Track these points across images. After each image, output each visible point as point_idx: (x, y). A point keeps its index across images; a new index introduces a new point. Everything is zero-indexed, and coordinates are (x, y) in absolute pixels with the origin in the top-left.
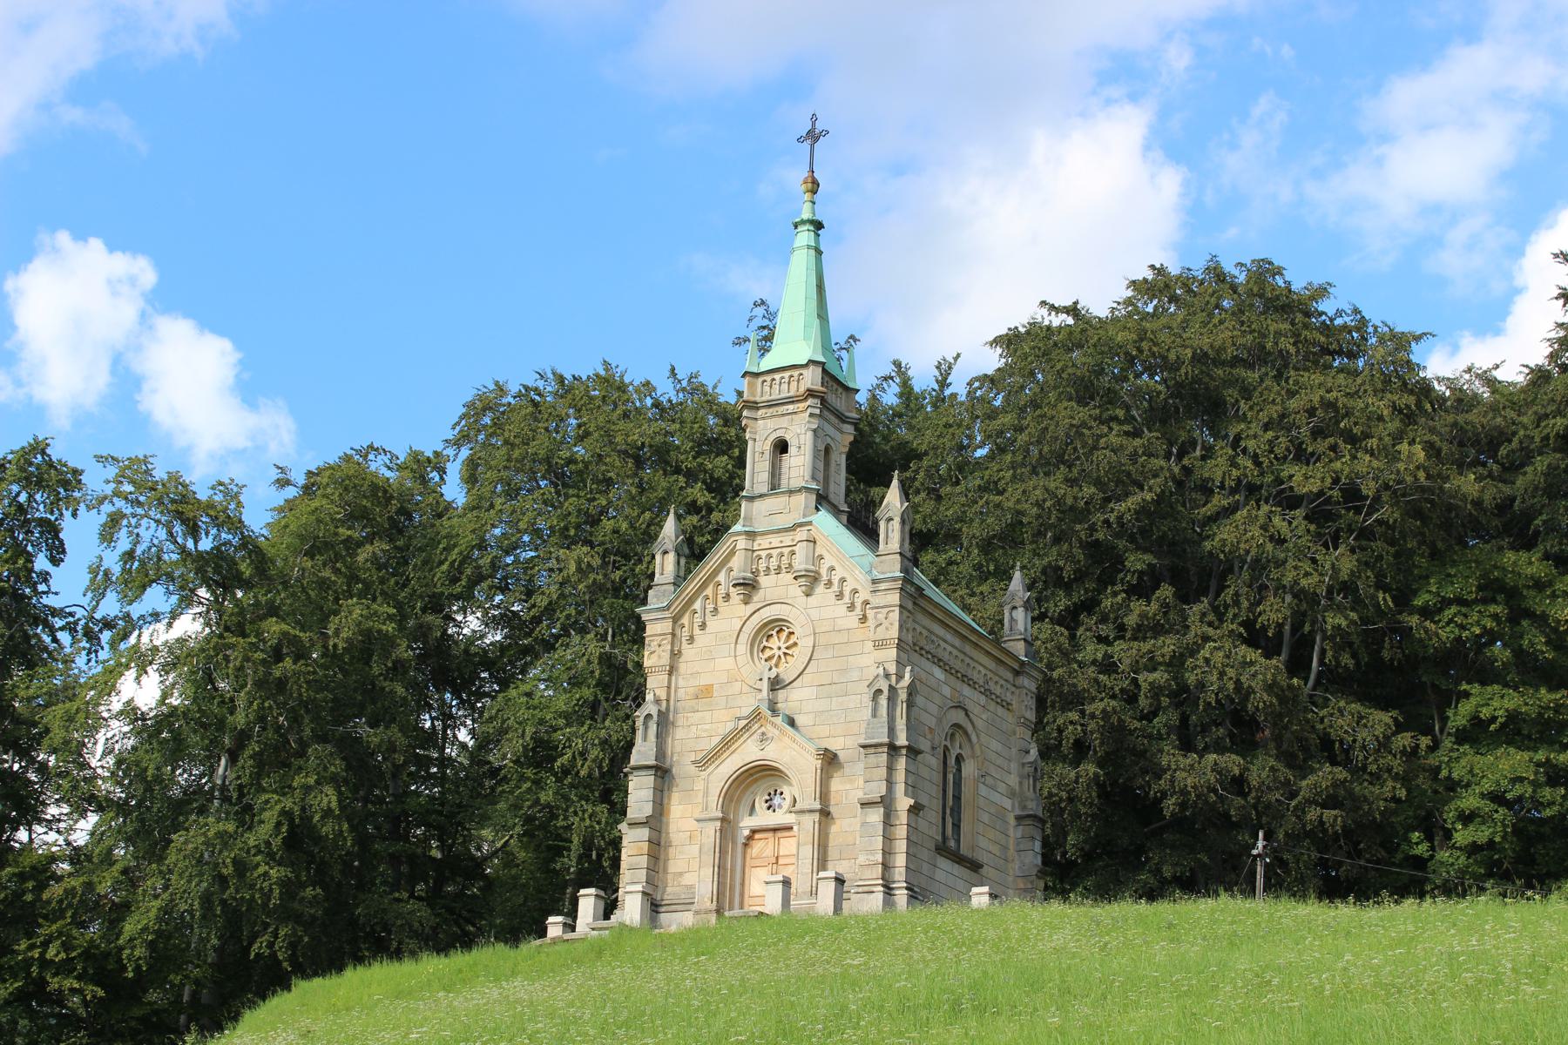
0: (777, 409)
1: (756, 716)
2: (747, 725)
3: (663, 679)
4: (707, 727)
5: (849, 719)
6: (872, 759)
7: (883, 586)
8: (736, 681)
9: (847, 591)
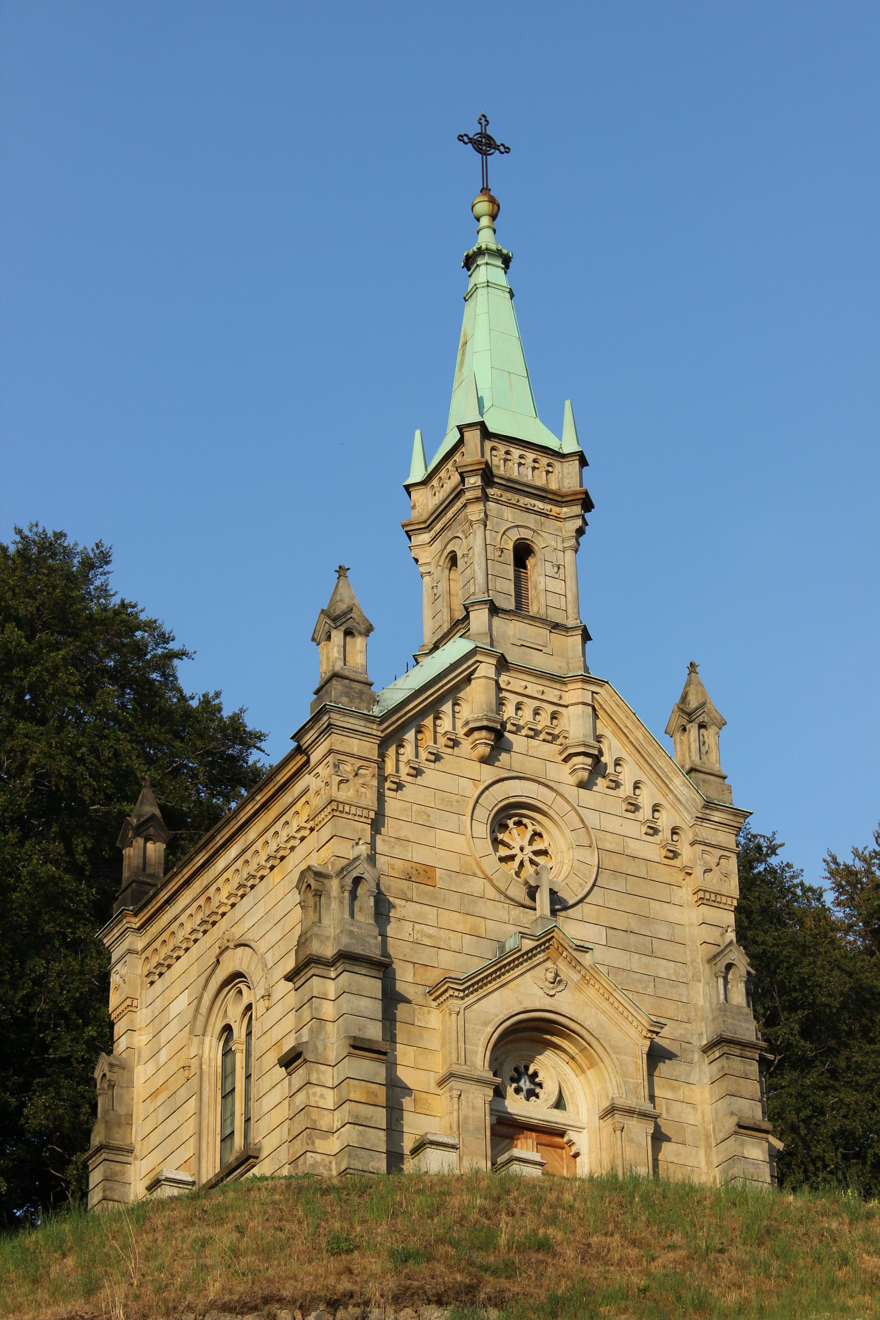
0: (517, 497)
2: (531, 950)
3: (363, 830)
4: (431, 931)
5: (660, 992)
6: (737, 1065)
7: (717, 816)
8: (474, 875)
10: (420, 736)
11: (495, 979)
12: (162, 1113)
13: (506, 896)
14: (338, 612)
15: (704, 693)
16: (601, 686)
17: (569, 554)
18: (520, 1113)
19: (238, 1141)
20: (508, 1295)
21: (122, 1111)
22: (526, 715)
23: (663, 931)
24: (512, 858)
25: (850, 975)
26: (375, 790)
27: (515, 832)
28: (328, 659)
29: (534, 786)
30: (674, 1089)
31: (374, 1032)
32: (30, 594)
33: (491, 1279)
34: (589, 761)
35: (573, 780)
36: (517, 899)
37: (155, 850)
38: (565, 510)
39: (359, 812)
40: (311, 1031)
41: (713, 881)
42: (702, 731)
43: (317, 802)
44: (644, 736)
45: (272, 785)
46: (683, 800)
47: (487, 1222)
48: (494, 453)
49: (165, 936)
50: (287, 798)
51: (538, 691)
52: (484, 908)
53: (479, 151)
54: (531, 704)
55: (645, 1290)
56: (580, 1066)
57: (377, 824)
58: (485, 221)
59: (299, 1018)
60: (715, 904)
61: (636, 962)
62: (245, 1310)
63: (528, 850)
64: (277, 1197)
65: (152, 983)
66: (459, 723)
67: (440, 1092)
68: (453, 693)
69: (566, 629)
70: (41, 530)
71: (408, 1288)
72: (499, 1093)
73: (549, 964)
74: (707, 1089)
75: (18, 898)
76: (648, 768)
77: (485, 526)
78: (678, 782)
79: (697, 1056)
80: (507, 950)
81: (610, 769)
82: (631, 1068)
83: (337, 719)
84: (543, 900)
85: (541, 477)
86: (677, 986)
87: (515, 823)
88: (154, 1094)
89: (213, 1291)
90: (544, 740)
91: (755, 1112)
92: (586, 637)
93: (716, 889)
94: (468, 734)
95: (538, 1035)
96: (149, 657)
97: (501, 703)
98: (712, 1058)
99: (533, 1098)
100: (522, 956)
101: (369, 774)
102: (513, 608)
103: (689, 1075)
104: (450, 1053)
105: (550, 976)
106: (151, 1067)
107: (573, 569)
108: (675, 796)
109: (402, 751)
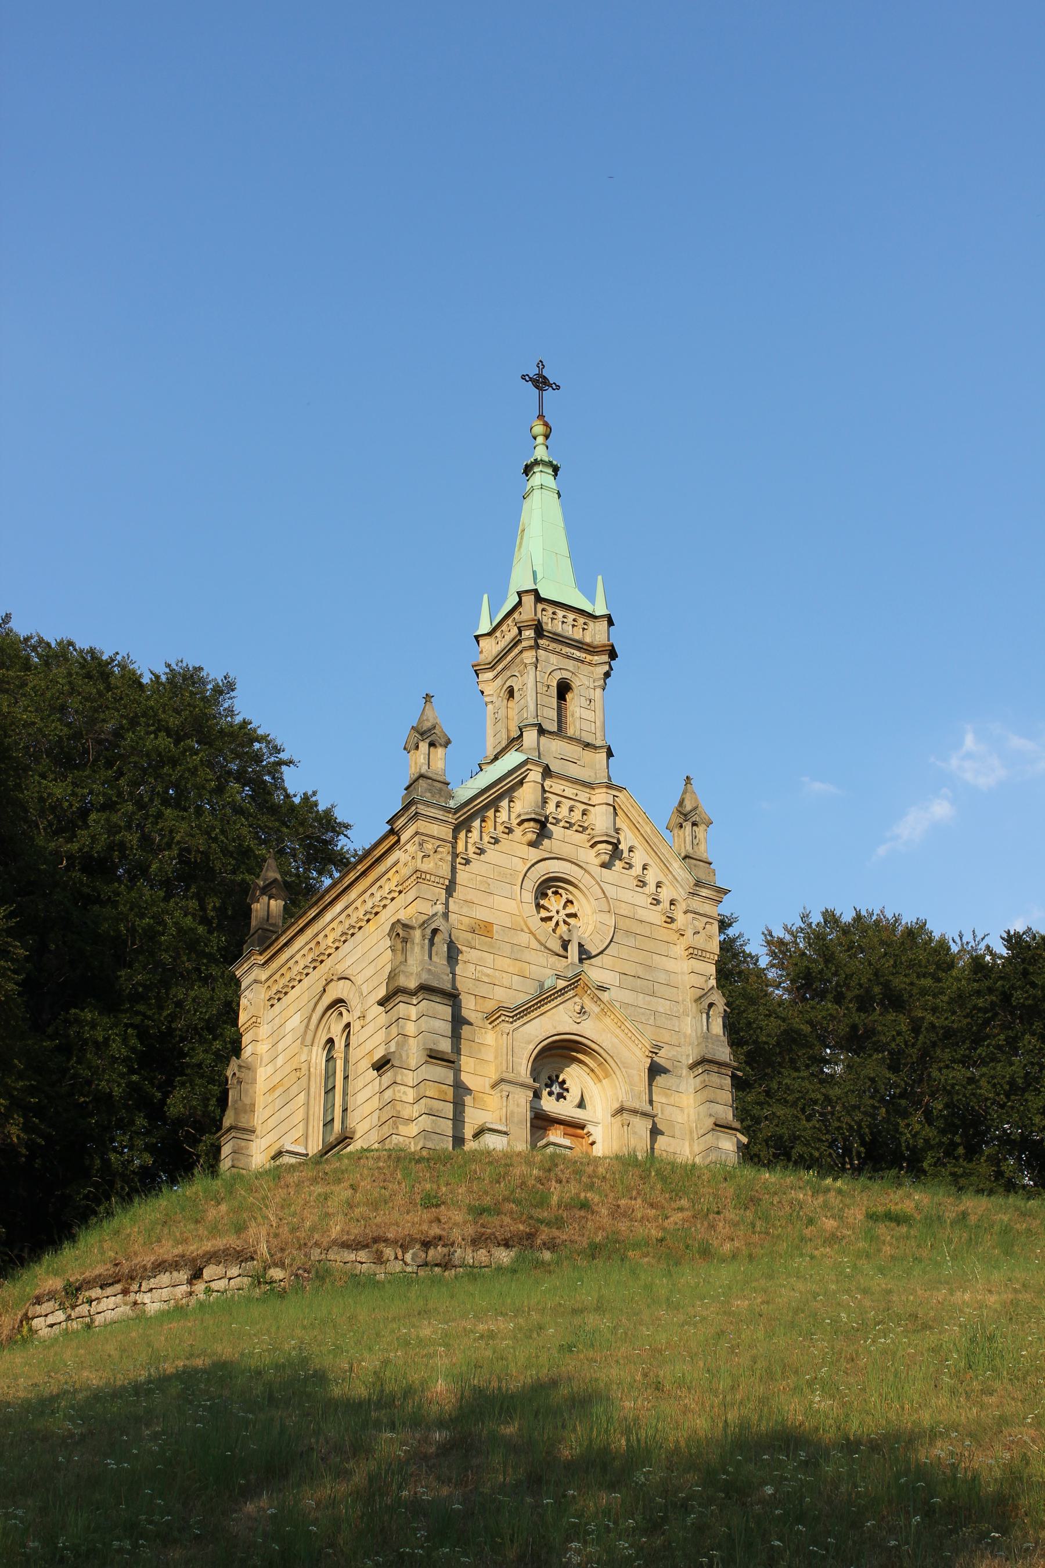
1: (575, 983)
2: (564, 988)
3: (440, 894)
5: (658, 1023)
6: (715, 1079)
7: (704, 892)
8: (522, 930)
9: (651, 878)
10: (483, 824)
11: (536, 1009)
12: (278, 1103)
13: (546, 947)
14: (425, 728)
15: (696, 799)
16: (620, 791)
17: (599, 691)
18: (552, 1110)
19: (337, 1125)
20: (558, 1241)
21: (247, 1101)
22: (564, 811)
23: (662, 978)
24: (550, 918)
25: (784, 1020)
26: (449, 863)
27: (553, 899)
28: (416, 763)
29: (568, 865)
30: (666, 1096)
31: (445, 1046)
32: (178, 712)
33: (546, 1229)
34: (610, 847)
35: (598, 861)
36: (554, 950)
37: (276, 905)
38: (596, 658)
39: (437, 880)
40: (397, 1043)
41: (700, 941)
42: (695, 828)
43: (405, 872)
44: (652, 830)
45: (370, 858)
46: (679, 879)
47: (541, 1187)
48: (544, 613)
49: (283, 970)
50: (381, 868)
51: (573, 794)
52: (529, 956)
53: (537, 387)
54: (566, 804)
55: (662, 1240)
56: (597, 1076)
57: (450, 889)
58: (540, 439)
59: (388, 1034)
60: (702, 958)
61: (641, 1000)
62: (359, 1247)
63: (563, 913)
64: (381, 1164)
65: (272, 1006)
66: (513, 816)
67: (493, 1093)
68: (509, 793)
69: (595, 747)
70: (185, 665)
71: (483, 1234)
72: (537, 1095)
73: (577, 999)
74: (692, 1096)
75: (165, 940)
76: (653, 854)
77: (536, 668)
78: (676, 866)
79: (685, 1072)
80: (546, 988)
81: (625, 854)
82: (636, 1079)
83: (422, 809)
84: (573, 951)
85: (579, 633)
86: (671, 1019)
87: (553, 893)
88: (273, 1089)
89: (335, 1231)
90: (576, 831)
91: (727, 1114)
92: (610, 754)
93: (702, 947)
94: (520, 824)
95: (566, 1051)
96: (264, 763)
97: (545, 801)
98: (696, 1073)
99: (562, 1100)
100: (557, 992)
101: (445, 850)
102: (556, 730)
103: (678, 1086)
104: (501, 1063)
105: (578, 1008)
106: (270, 1069)
107: (601, 702)
108: (674, 876)
109: (470, 835)
